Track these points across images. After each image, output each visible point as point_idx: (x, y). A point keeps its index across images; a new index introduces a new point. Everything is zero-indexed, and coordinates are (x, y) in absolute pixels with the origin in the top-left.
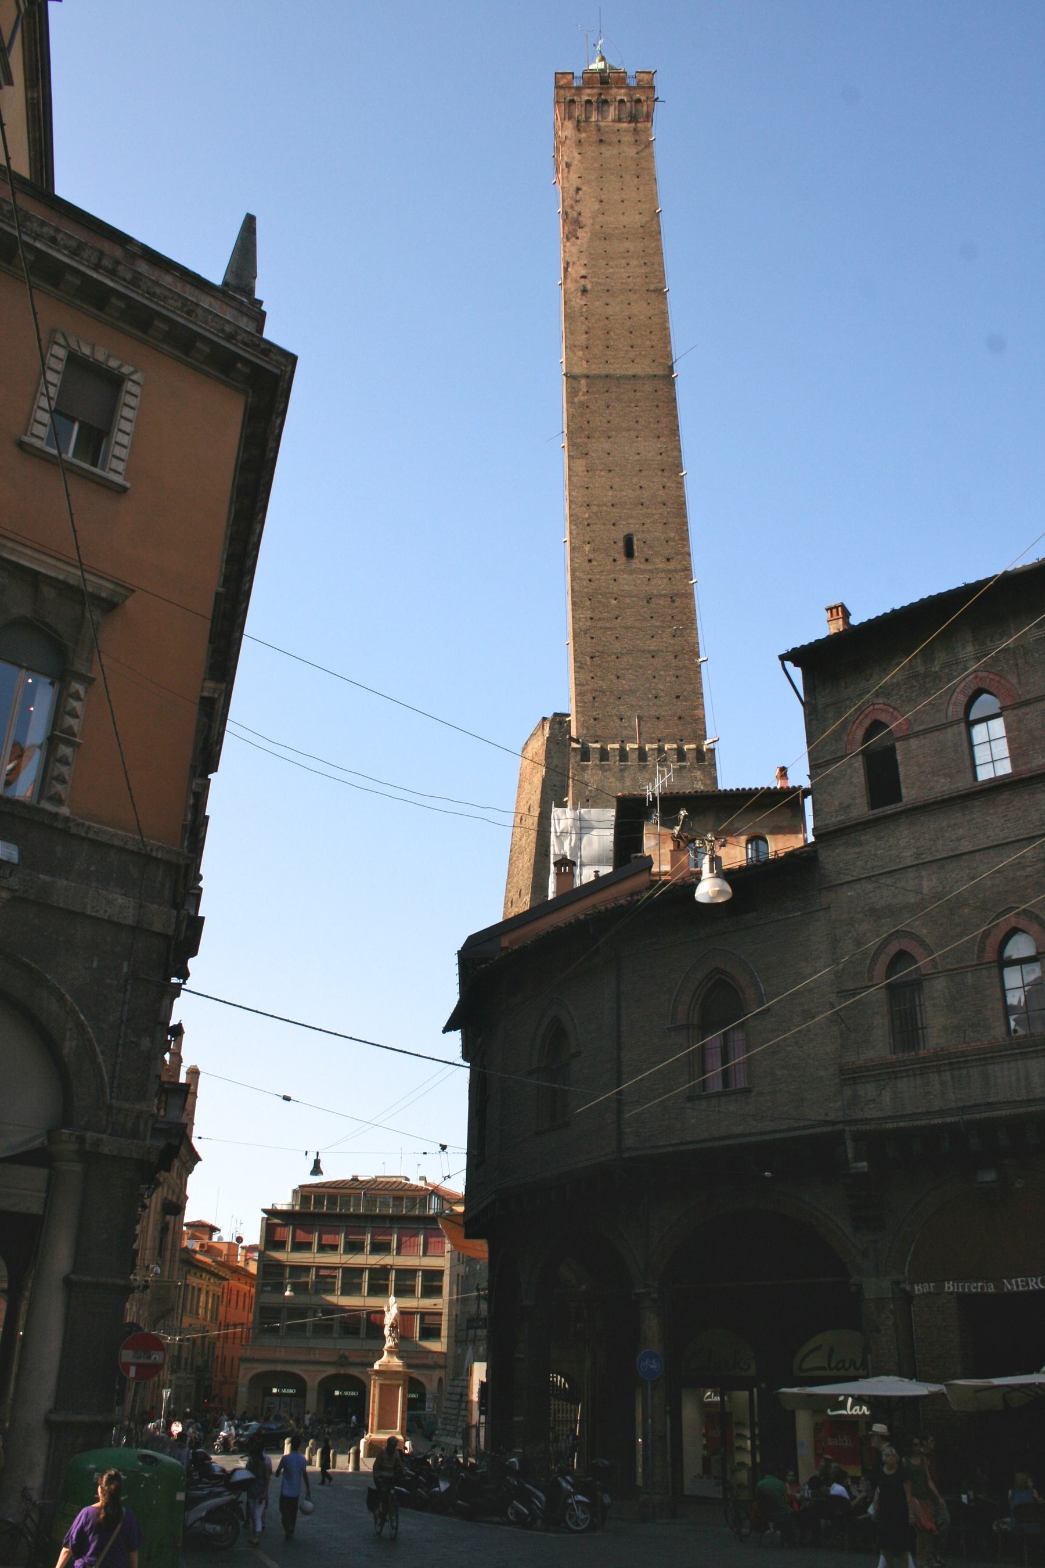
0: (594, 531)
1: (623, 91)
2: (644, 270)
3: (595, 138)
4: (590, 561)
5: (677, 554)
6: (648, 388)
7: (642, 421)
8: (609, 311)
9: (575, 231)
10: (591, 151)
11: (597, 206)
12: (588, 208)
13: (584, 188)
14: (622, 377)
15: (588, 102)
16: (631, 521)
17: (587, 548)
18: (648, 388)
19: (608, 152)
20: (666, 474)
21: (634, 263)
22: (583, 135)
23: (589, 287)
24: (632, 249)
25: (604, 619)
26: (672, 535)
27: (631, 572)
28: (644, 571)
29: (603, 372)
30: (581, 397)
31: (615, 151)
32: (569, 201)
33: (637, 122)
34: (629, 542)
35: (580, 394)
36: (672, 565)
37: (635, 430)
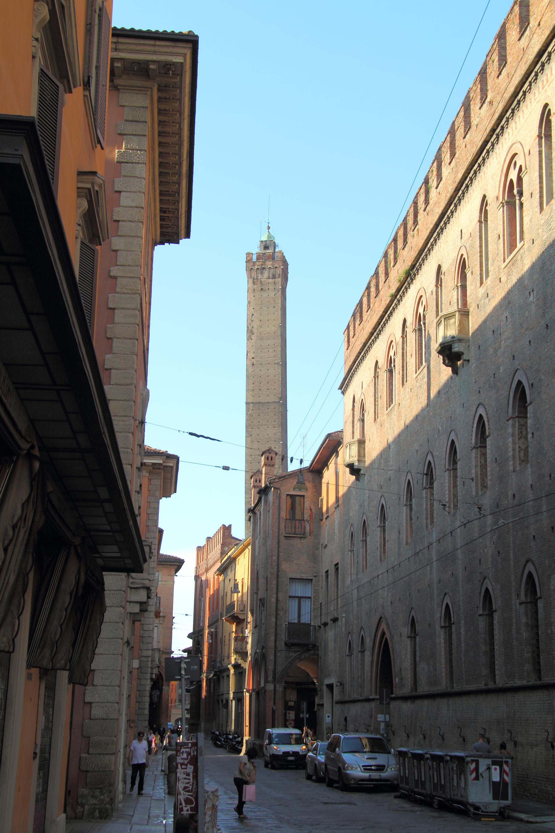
1: (271, 263)
3: (260, 288)
6: (272, 407)
7: (270, 422)
9: (251, 336)
12: (256, 324)
14: (263, 403)
15: (258, 268)
19: (265, 295)
21: (270, 351)
22: (255, 286)
23: (255, 363)
29: (258, 401)
30: (250, 412)
31: (266, 295)
32: (249, 321)
33: (275, 278)
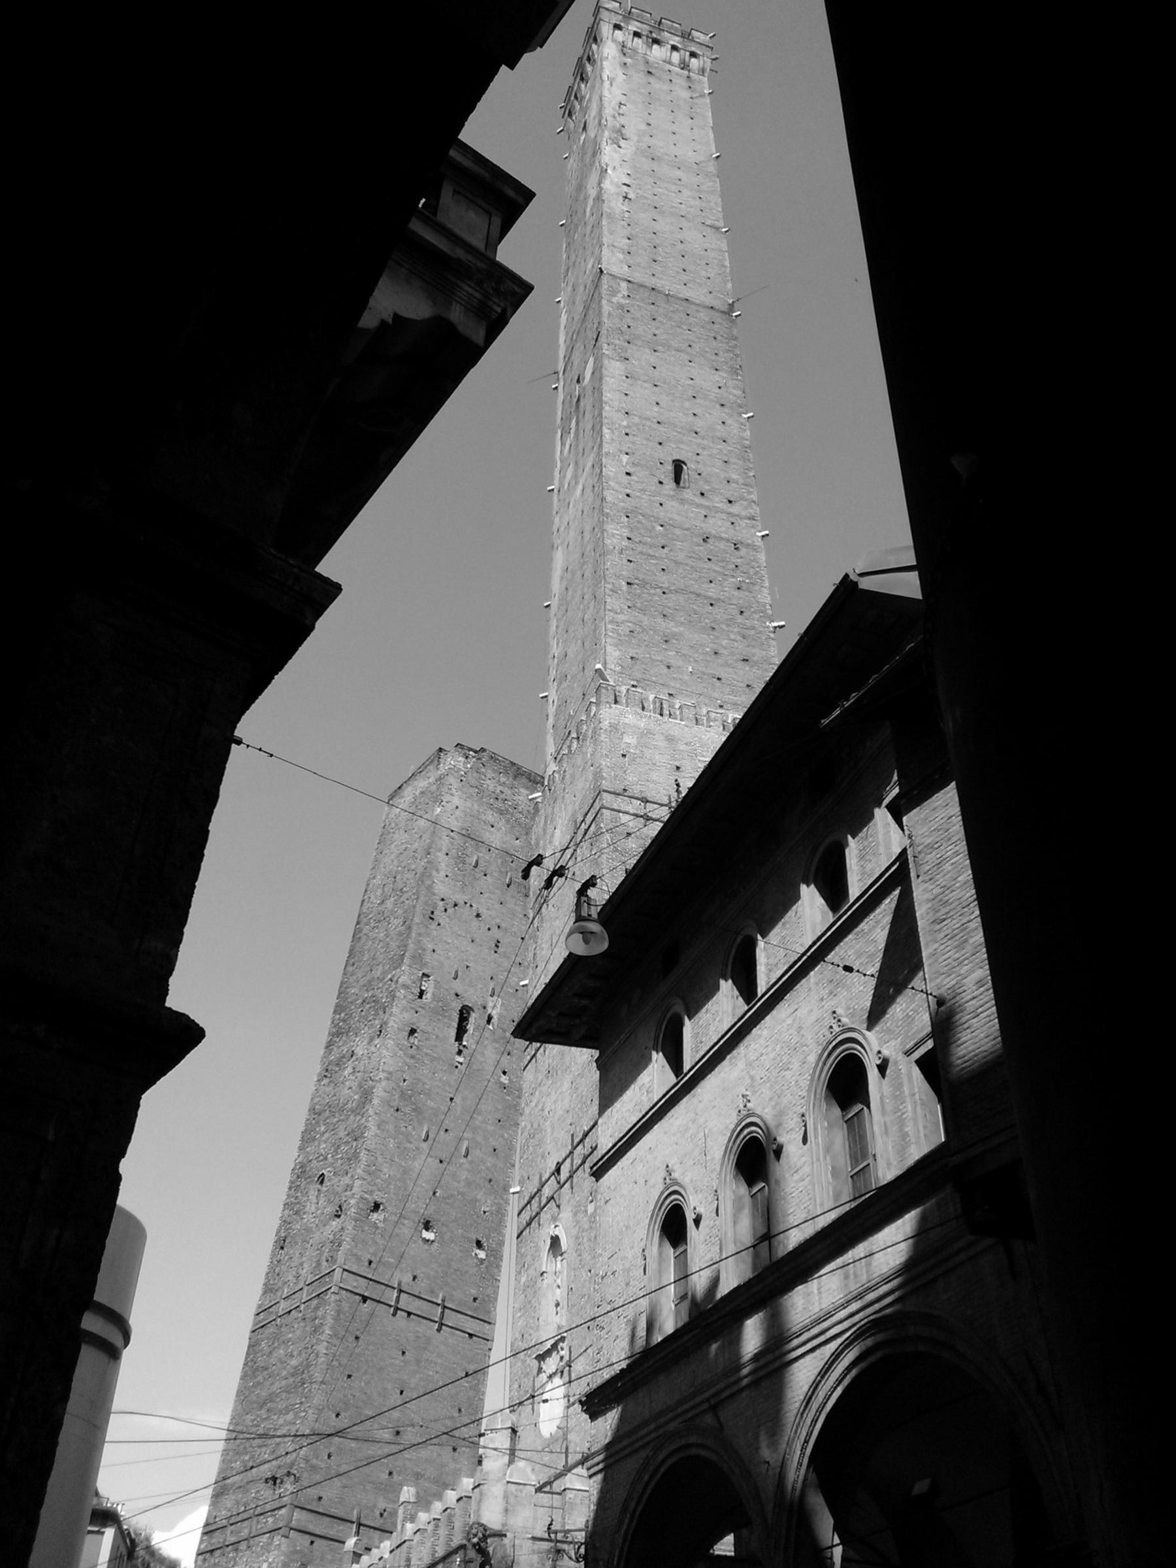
0: (633, 443)
2: (697, 202)
4: (628, 474)
5: (742, 499)
7: (696, 347)
8: (657, 227)
10: (639, 78)
11: (644, 127)
13: (629, 106)
16: (682, 446)
17: (625, 458)
18: (704, 316)
19: (657, 85)
20: (726, 410)
21: (685, 192)
22: (628, 61)
24: (684, 179)
25: (645, 544)
26: (735, 476)
27: (683, 501)
28: (698, 506)
34: (678, 466)
35: (620, 295)
36: (734, 509)
37: (688, 353)
